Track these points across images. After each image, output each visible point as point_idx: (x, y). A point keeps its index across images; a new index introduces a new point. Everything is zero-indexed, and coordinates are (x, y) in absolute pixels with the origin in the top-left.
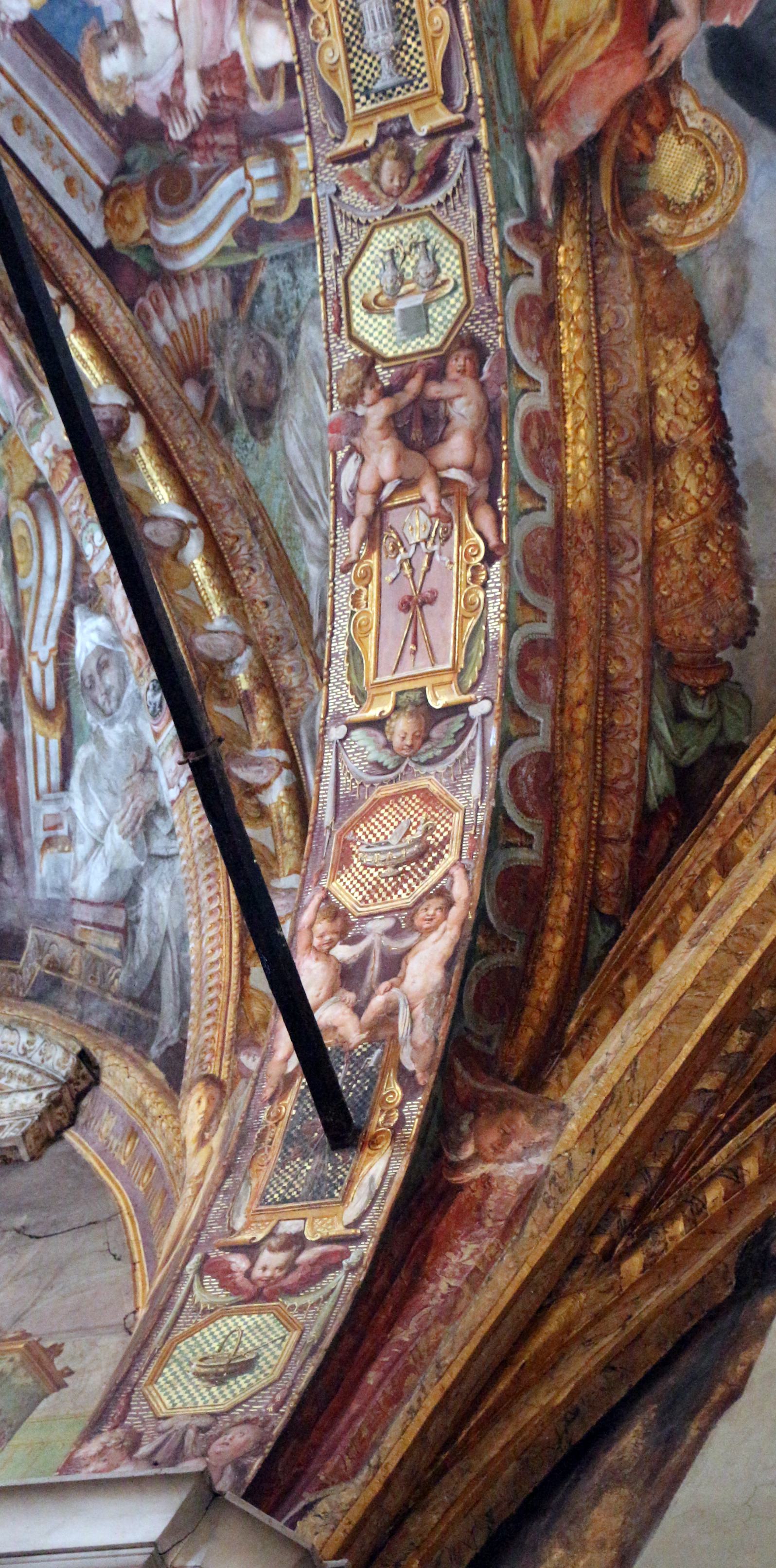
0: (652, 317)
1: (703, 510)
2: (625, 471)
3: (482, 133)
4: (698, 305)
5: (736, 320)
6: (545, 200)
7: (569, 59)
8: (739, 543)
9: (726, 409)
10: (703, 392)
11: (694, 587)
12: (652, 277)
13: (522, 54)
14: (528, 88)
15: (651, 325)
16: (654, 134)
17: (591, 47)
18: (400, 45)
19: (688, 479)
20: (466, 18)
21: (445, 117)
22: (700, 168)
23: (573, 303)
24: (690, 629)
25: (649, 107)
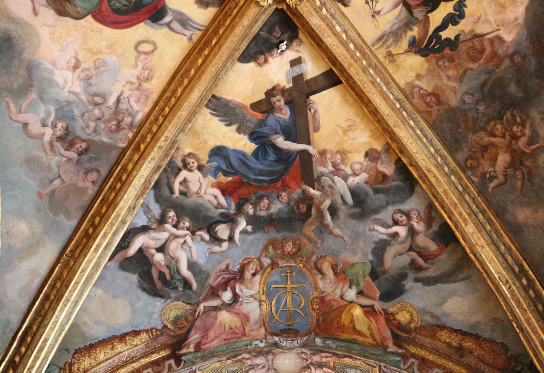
0: (432, 335)
1: (475, 344)
2: (461, 357)
3: (383, 364)
4: (432, 325)
5: (438, 318)
6: (400, 351)
7: (375, 332)
8: (485, 339)
9: (456, 328)
10: (450, 331)
11: (492, 354)
12: (423, 332)
13: (370, 344)
14: (377, 346)
15: (433, 336)
16: (395, 319)
17: (374, 325)
18: (361, 370)
19: (468, 344)
20: (360, 358)
21: (377, 369)
22: (405, 312)
23: (423, 353)
24: (501, 360)
25: (389, 318)
